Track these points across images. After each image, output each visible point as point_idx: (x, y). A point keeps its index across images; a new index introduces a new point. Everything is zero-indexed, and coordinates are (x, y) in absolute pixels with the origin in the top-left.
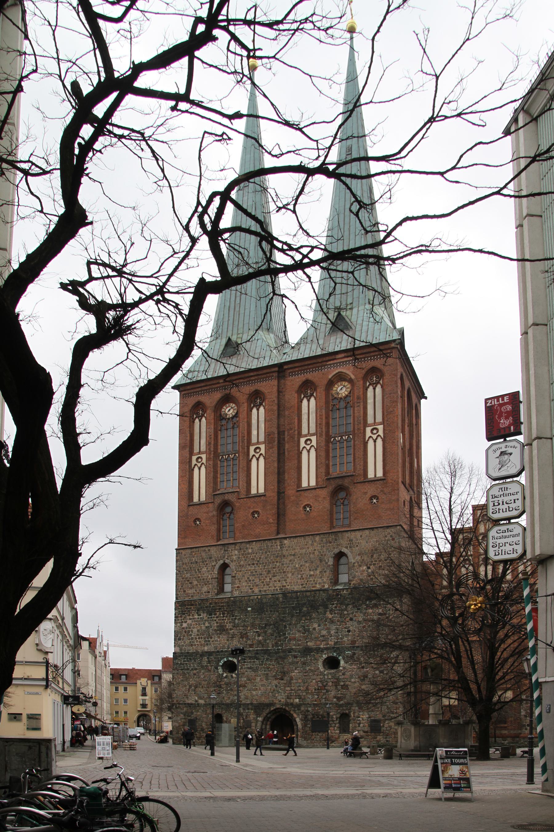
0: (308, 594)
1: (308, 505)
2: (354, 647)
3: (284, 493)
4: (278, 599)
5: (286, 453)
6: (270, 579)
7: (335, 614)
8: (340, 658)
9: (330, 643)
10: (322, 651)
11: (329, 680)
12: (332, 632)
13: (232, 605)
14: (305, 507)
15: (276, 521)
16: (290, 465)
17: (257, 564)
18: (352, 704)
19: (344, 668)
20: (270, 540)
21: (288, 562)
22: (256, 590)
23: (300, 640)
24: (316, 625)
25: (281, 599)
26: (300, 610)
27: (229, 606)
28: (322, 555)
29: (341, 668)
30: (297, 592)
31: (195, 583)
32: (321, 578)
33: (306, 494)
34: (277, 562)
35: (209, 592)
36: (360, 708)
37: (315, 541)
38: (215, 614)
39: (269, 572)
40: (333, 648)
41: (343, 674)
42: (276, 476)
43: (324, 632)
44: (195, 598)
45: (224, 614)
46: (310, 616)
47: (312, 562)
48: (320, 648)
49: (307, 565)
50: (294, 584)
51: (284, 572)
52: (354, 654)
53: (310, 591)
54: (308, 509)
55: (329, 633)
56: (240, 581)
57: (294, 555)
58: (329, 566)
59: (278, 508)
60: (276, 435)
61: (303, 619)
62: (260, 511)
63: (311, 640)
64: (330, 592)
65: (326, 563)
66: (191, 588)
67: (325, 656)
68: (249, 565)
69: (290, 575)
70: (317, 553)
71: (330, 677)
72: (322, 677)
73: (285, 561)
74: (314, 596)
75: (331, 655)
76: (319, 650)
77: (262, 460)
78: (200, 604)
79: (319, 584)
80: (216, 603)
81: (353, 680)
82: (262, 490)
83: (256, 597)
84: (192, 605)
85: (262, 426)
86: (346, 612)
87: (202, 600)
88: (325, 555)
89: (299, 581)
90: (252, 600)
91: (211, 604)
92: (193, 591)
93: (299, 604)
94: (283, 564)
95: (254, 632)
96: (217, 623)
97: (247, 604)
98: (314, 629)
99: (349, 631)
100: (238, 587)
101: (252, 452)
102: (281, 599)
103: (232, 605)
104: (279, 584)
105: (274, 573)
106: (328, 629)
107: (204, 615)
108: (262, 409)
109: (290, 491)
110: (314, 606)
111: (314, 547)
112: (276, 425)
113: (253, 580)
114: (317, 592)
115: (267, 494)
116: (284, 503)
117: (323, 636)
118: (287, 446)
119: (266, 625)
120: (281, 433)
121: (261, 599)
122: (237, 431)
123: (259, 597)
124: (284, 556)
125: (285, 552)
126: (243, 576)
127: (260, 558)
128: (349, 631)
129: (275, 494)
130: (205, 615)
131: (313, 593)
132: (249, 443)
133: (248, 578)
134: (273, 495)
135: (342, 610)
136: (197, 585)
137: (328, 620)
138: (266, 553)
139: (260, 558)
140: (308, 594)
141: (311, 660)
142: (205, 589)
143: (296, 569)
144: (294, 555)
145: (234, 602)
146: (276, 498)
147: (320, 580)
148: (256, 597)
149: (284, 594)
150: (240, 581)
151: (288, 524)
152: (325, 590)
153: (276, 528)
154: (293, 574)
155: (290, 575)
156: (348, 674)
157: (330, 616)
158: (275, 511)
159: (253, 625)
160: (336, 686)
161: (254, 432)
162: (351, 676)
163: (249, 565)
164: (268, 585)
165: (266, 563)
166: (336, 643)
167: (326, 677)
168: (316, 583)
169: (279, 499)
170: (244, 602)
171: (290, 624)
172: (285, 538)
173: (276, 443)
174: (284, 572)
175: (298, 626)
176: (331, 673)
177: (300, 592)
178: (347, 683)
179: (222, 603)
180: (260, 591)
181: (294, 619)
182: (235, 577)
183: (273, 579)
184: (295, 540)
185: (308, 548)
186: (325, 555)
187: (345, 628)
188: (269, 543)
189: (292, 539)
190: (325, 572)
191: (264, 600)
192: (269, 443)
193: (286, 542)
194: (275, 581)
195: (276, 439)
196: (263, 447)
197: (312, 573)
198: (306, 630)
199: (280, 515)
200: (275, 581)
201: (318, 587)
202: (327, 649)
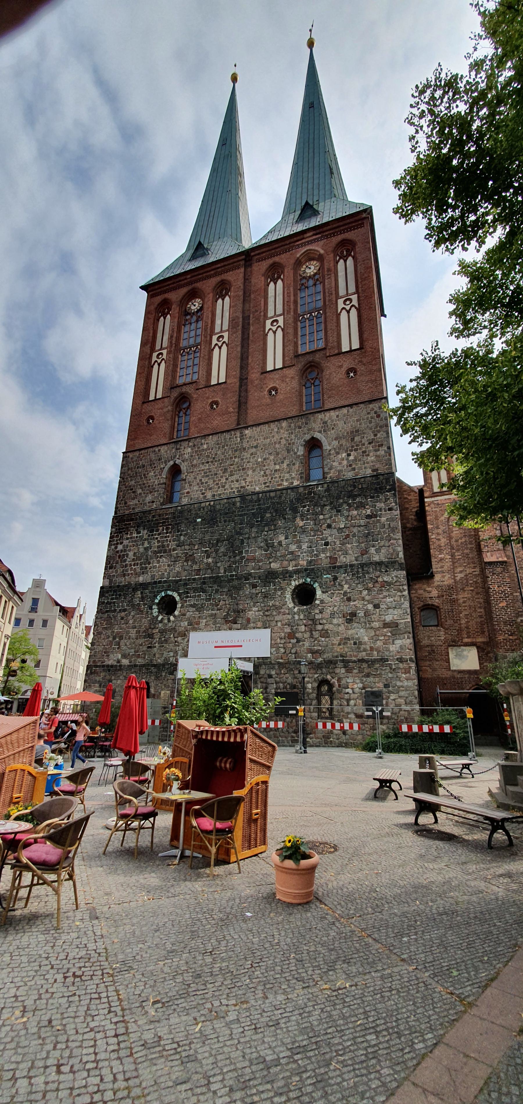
0: (272, 494)
1: (275, 389)
2: (334, 567)
3: (247, 379)
4: (234, 504)
5: (251, 335)
6: (227, 479)
7: (307, 519)
8: (316, 585)
9: (301, 562)
10: (291, 576)
11: (301, 623)
12: (305, 546)
13: (179, 517)
14: (270, 392)
15: (236, 410)
16: (252, 347)
17: (212, 462)
18: (335, 663)
19: (322, 602)
20: (228, 431)
21: (249, 456)
22: (209, 495)
23: (261, 561)
24: (282, 538)
25: (238, 504)
26: (262, 518)
27: (174, 518)
28: (289, 444)
29: (317, 602)
30: (258, 493)
31: (139, 491)
32: (289, 472)
33: (272, 375)
34: (235, 457)
35: (153, 502)
36: (349, 670)
37: (282, 427)
38: (157, 530)
39: (226, 469)
40: (306, 570)
41: (321, 612)
42: (239, 361)
43: (293, 547)
44: (137, 510)
45: (167, 529)
46: (275, 525)
47: (278, 454)
48: (287, 572)
49: (272, 458)
50: (255, 482)
51: (243, 469)
52: (335, 578)
53: (275, 491)
54: (273, 393)
55: (300, 547)
56: (190, 485)
57: (256, 447)
58: (299, 456)
59: (240, 396)
60: (241, 320)
61: (266, 529)
62: (219, 400)
63: (276, 559)
64: (301, 490)
65: (295, 453)
66: (133, 499)
67: (293, 583)
68: (203, 463)
69: (250, 472)
70: (283, 442)
71: (302, 617)
72: (290, 617)
73: (246, 455)
74: (280, 497)
75: (301, 581)
76: (287, 575)
77: (224, 348)
78: (141, 518)
79: (287, 480)
80: (160, 515)
81: (335, 621)
82: (222, 380)
83: (208, 503)
84: (132, 520)
85: (227, 314)
86: (321, 517)
87: (144, 513)
88: (294, 443)
89: (261, 479)
90: (203, 508)
91: (154, 516)
92: (135, 501)
93: (260, 509)
94: (242, 459)
95: (202, 552)
96: (158, 542)
97: (197, 514)
98: (280, 543)
99: (327, 544)
100: (188, 493)
101: (214, 341)
102: (238, 504)
103: (179, 517)
104: (237, 485)
105: (231, 471)
106: (299, 542)
107: (144, 533)
108: (227, 299)
109: (254, 375)
110: (280, 513)
111: (280, 434)
112: (241, 309)
113: (206, 483)
114: (284, 491)
115: (228, 381)
116: (246, 391)
117: (292, 553)
118: (252, 328)
119: (218, 541)
120: (246, 319)
121: (214, 506)
122: (200, 324)
123: (212, 503)
124: (244, 449)
125: (245, 445)
126: (195, 478)
127: (216, 454)
128: (327, 544)
129: (237, 381)
130: (146, 531)
131: (278, 493)
132: (212, 333)
133: (201, 480)
134: (235, 381)
135: (317, 514)
136: (140, 494)
137: (298, 530)
138: (223, 447)
139: (216, 454)
140: (272, 494)
141: (275, 589)
142: (149, 498)
143: (258, 463)
144: (256, 447)
145: (181, 512)
146: (238, 384)
147: (287, 476)
148: (208, 503)
149: (243, 497)
150: (190, 485)
151: (249, 411)
152: (293, 489)
153: (236, 418)
154: (254, 471)
155: (250, 472)
156: (328, 611)
157: (301, 523)
158: (235, 398)
159: (201, 544)
160: (311, 631)
161: (218, 322)
162: (333, 615)
163: (203, 463)
164: (223, 487)
165: (222, 460)
166: (310, 563)
167: (296, 617)
168: (282, 480)
169: (241, 386)
170: (193, 512)
171: (249, 538)
172: (246, 428)
173: (240, 327)
174: (243, 469)
175: (259, 540)
176: (303, 611)
177: (263, 492)
178: (326, 627)
179: (166, 514)
180: (214, 496)
181: (254, 530)
182: (185, 480)
183: (231, 479)
184: (258, 429)
185: (273, 436)
186: (294, 443)
187: (322, 539)
188: (227, 436)
189: (254, 428)
190: (294, 464)
191: (218, 507)
192: (233, 328)
193: (247, 432)
194: (232, 481)
195: (241, 323)
196: (226, 335)
197: (277, 467)
198: (269, 546)
199: (242, 404)
200: (232, 481)
201: (285, 484)
202: (297, 572)
